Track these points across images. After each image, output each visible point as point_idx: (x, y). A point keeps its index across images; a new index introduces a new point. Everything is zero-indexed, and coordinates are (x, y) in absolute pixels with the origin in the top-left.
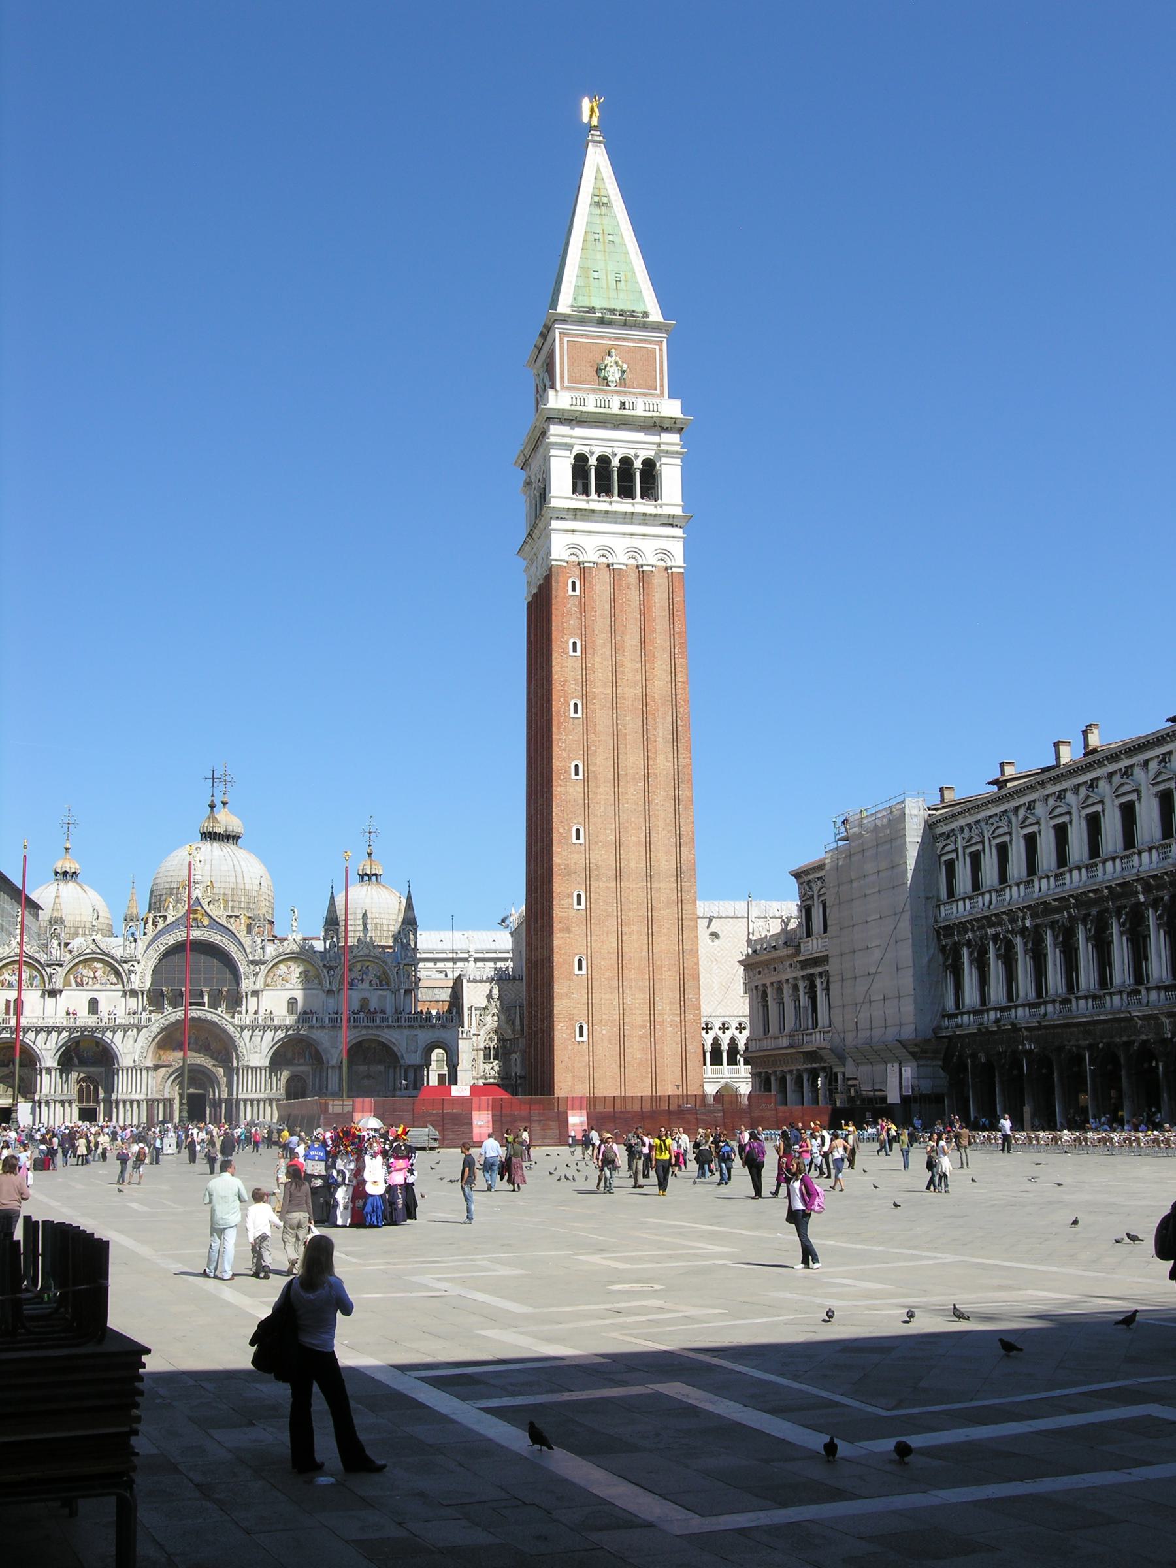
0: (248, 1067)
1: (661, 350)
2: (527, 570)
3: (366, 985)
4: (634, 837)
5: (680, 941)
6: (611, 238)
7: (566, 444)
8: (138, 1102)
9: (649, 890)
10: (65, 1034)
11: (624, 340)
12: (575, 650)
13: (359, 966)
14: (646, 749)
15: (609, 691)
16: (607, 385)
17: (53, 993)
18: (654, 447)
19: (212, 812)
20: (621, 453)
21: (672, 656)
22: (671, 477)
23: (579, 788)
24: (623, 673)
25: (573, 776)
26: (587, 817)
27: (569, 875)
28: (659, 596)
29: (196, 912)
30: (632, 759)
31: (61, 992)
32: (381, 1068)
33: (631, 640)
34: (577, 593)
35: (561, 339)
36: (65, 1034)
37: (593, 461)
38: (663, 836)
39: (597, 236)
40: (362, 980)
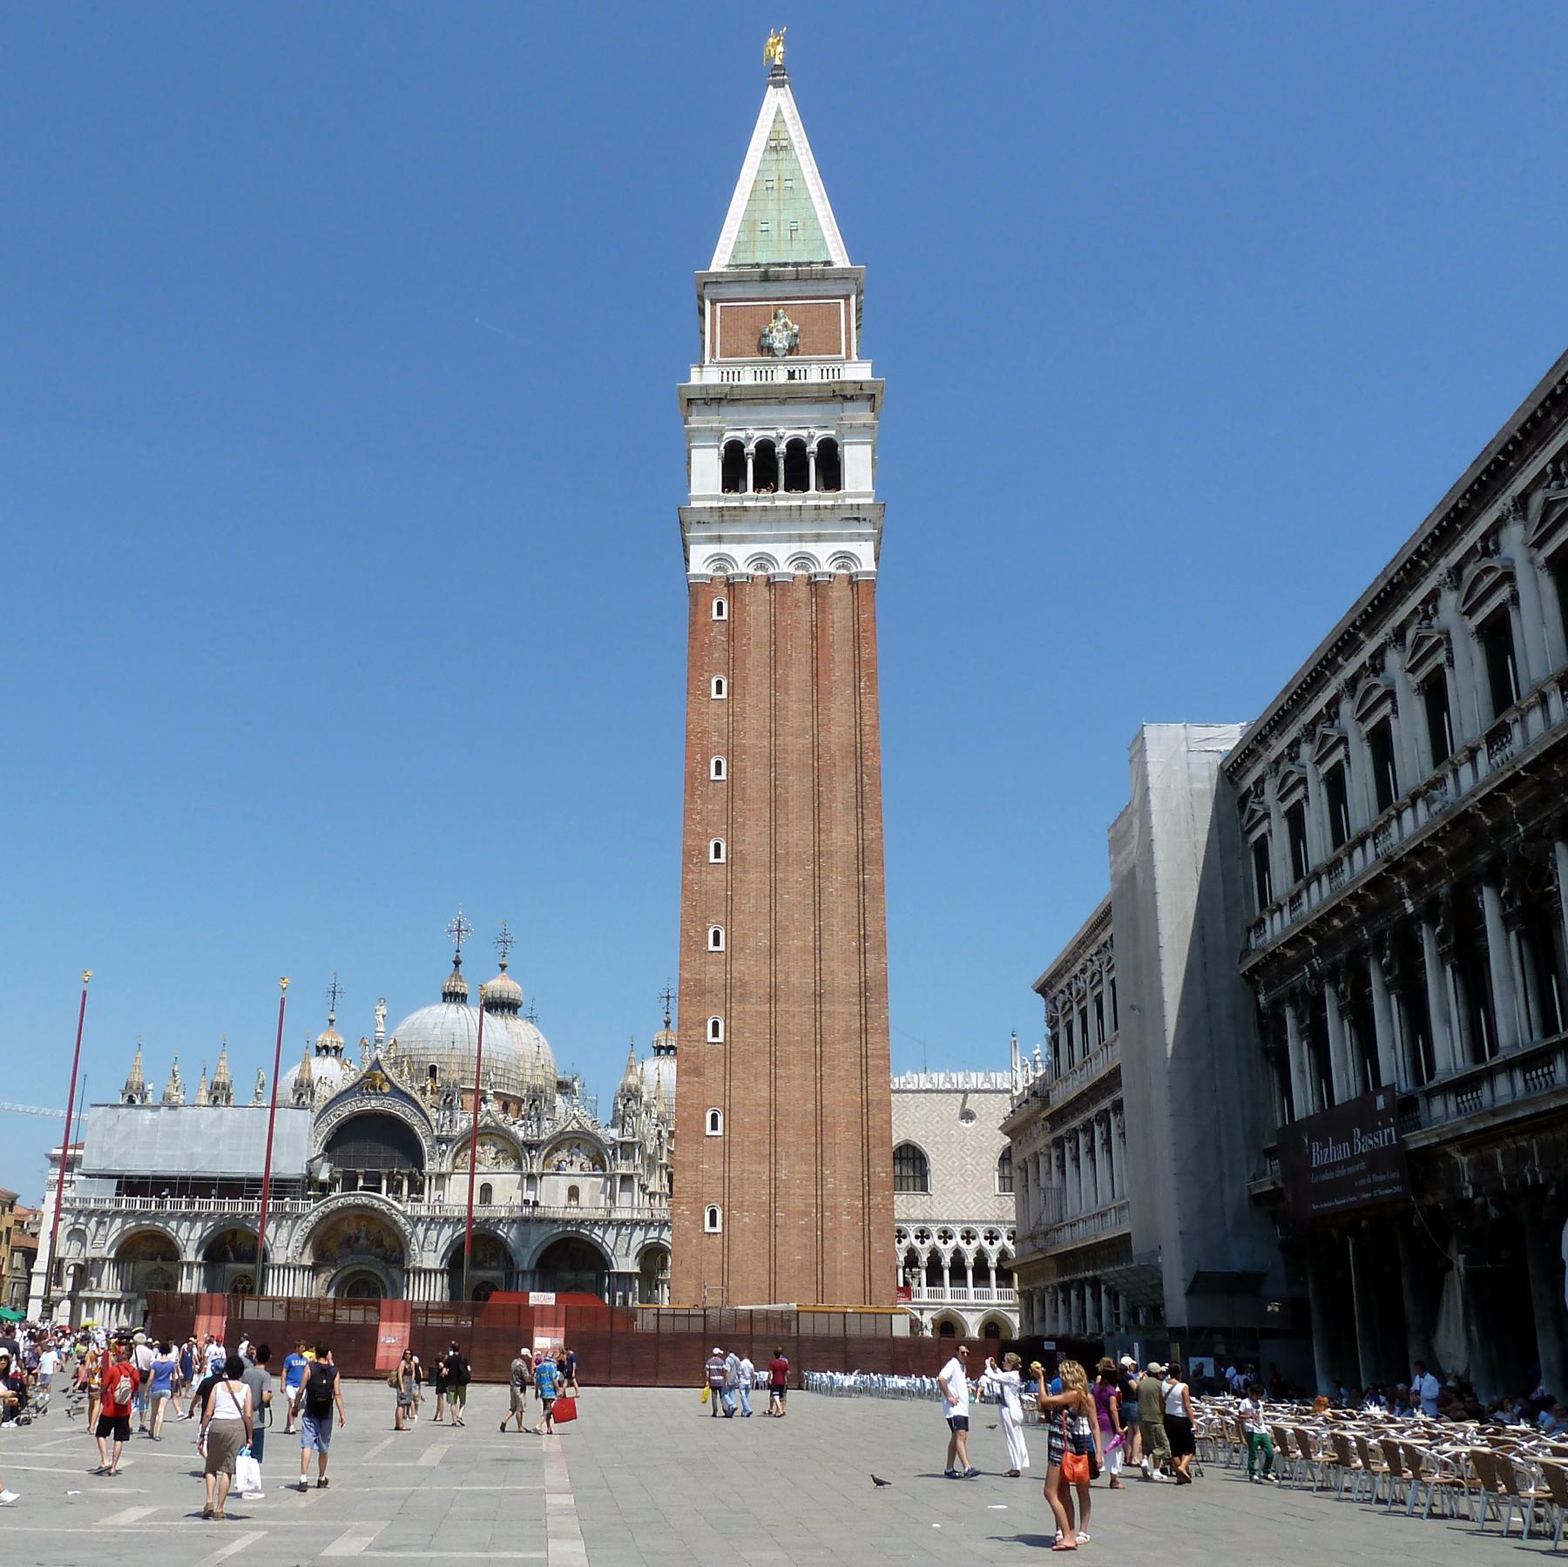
3: (576, 1170)
4: (797, 941)
5: (864, 1089)
9: (817, 1015)
12: (719, 691)
14: (816, 819)
15: (766, 743)
16: (774, 355)
22: (857, 464)
23: (720, 875)
24: (786, 718)
25: (712, 859)
26: (730, 915)
27: (702, 993)
29: (374, 1077)
30: (797, 833)
32: (592, 1276)
33: (798, 675)
34: (725, 617)
38: (840, 939)
40: (571, 1163)
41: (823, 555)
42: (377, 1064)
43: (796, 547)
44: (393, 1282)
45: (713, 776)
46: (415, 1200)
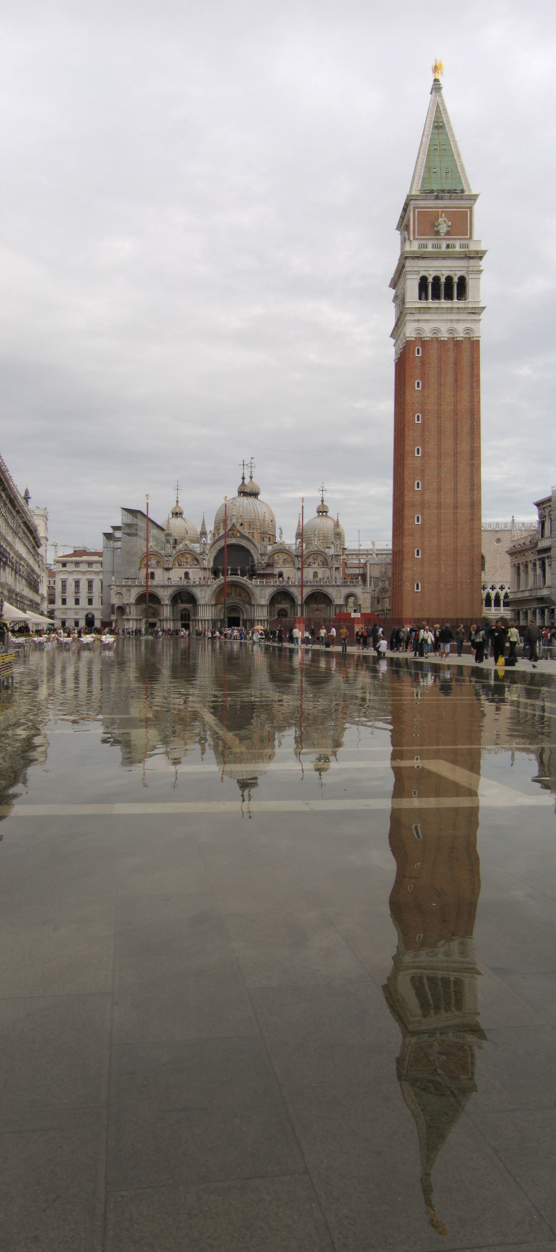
1: (471, 212)
2: (395, 345)
3: (316, 565)
6: (444, 147)
7: (416, 271)
8: (208, 620)
9: (455, 514)
10: (173, 589)
11: (450, 208)
12: (418, 387)
14: (456, 438)
15: (436, 408)
17: (168, 569)
19: (243, 481)
20: (446, 274)
23: (419, 461)
28: (466, 354)
30: (448, 445)
31: (171, 569)
32: (324, 606)
33: (449, 380)
36: (173, 589)
37: (430, 280)
39: (436, 147)
42: (234, 525)
43: (449, 325)
44: (246, 610)
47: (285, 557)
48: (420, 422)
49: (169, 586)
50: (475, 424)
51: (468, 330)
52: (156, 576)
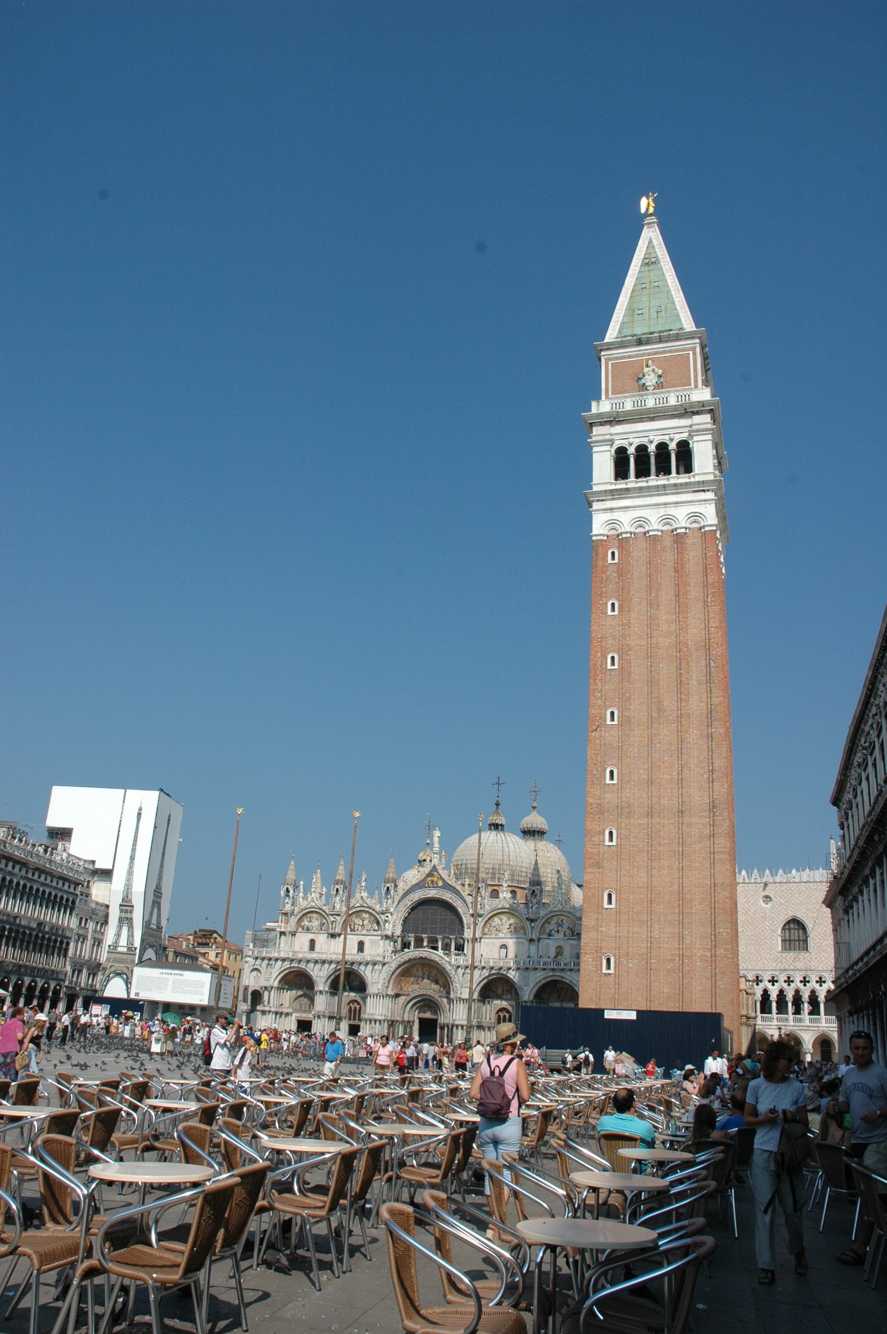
0: (460, 999)
1: (694, 354)
3: (561, 936)
5: (712, 875)
6: (656, 284)
7: (605, 441)
8: (380, 1021)
10: (333, 966)
11: (662, 353)
12: (613, 609)
13: (555, 920)
16: (647, 389)
17: (333, 936)
18: (687, 429)
21: (706, 605)
25: (609, 722)
27: (601, 812)
28: (693, 554)
33: (666, 595)
35: (607, 364)
36: (333, 966)
37: (631, 450)
39: (644, 286)
40: (558, 931)
41: (681, 517)
42: (434, 868)
43: (662, 511)
45: (609, 667)
46: (456, 955)
47: (512, 921)
48: (616, 667)
49: (324, 962)
50: (712, 664)
51: (695, 516)
52: (317, 947)
